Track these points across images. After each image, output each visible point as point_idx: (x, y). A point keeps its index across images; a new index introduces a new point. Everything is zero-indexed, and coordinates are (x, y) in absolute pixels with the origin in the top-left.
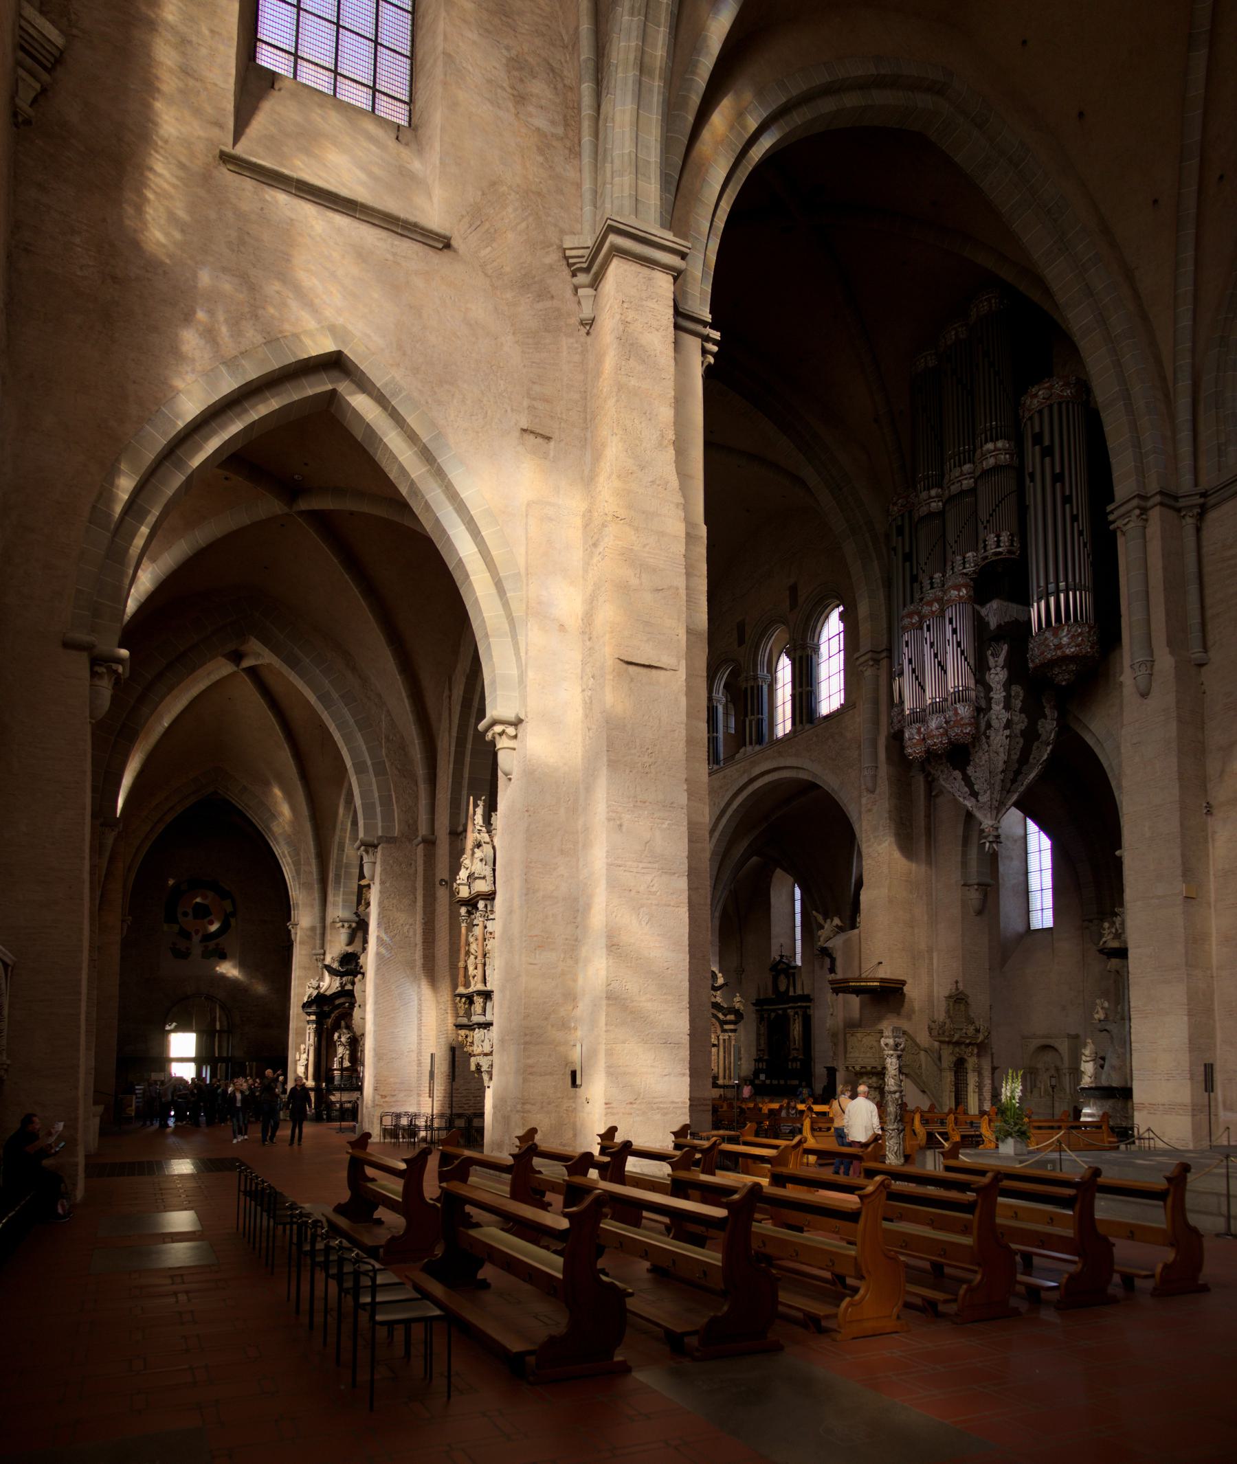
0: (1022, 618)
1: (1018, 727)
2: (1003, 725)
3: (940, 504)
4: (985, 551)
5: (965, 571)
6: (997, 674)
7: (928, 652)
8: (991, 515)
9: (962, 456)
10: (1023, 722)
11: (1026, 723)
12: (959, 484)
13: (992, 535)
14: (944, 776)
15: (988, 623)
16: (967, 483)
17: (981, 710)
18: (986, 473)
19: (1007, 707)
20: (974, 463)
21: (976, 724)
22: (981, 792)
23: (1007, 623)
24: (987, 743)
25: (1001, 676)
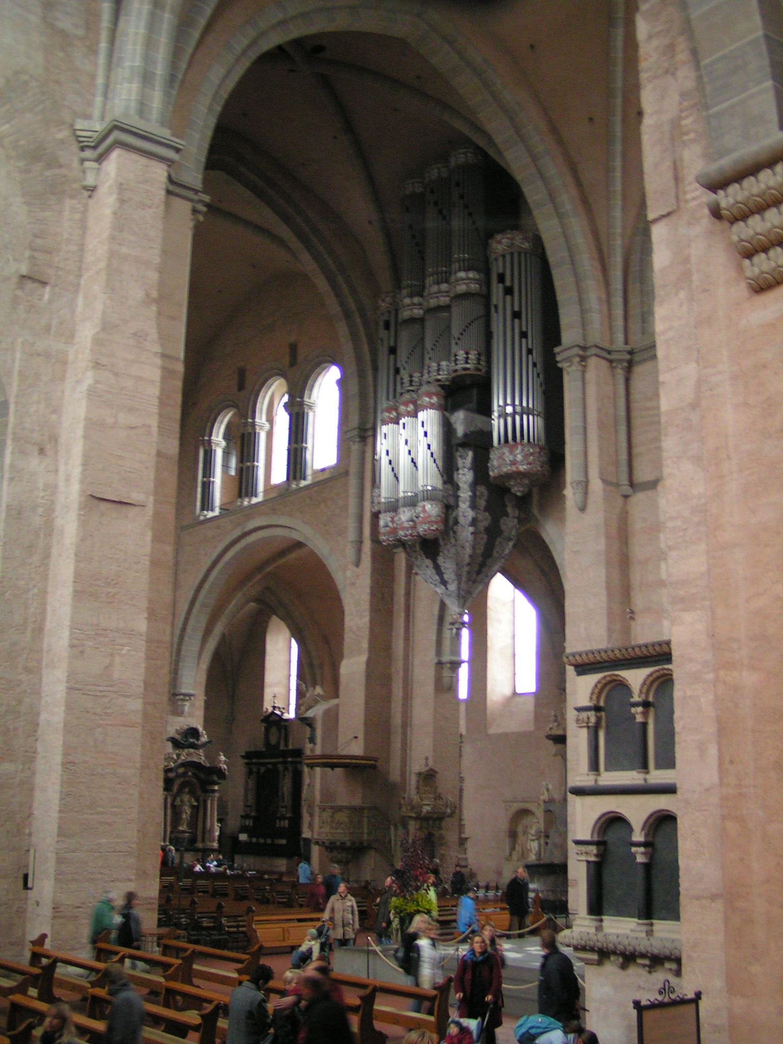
0: (486, 429)
3: (421, 312)
5: (439, 377)
6: (464, 474)
16: (444, 300)
17: (449, 508)
19: (473, 506)
22: (450, 581)
23: (473, 433)
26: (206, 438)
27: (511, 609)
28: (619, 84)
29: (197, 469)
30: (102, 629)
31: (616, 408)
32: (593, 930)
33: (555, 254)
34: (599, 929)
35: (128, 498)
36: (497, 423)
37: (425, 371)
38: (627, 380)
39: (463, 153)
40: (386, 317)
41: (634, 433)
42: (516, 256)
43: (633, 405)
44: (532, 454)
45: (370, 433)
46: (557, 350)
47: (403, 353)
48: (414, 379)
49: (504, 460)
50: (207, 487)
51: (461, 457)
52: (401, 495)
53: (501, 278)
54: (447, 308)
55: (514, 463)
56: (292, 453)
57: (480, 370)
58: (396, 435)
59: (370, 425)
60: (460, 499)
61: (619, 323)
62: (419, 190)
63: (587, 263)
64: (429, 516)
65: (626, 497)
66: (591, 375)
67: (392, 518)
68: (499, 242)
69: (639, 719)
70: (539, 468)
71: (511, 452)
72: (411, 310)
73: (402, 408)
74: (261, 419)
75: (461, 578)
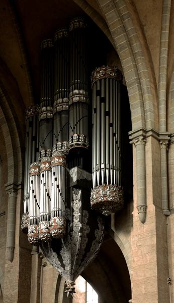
1: (86, 232)
5: (62, 150)
8: (76, 125)
10: (88, 230)
12: (61, 107)
13: (75, 135)
14: (49, 255)
15: (72, 178)
17: (68, 221)
18: (74, 104)
19: (81, 221)
20: (69, 98)
22: (67, 265)
36: (95, 176)
38: (167, 152)
40: (31, 120)
43: (170, 166)
44: (115, 191)
45: (20, 187)
46: (130, 133)
48: (47, 152)
51: (75, 193)
53: (99, 93)
55: (105, 196)
57: (86, 146)
59: (20, 183)
60: (74, 217)
65: (167, 216)
71: (103, 190)
75: (73, 264)
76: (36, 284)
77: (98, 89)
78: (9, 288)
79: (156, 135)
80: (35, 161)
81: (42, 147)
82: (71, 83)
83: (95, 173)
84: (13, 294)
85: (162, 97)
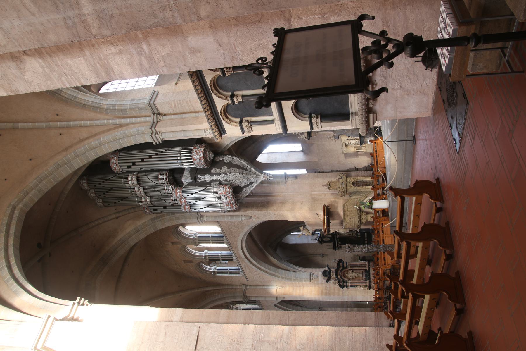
0: (189, 170)
1: (226, 170)
2: (226, 175)
3: (147, 197)
4: (165, 183)
5: (171, 190)
6: (207, 178)
7: (199, 203)
8: (153, 181)
9: (132, 191)
11: (225, 167)
13: (160, 181)
15: (190, 182)
16: (141, 189)
19: (219, 174)
21: (226, 185)
24: (232, 181)
25: (208, 176)
26: (213, 273)
27: (271, 154)
28: (44, 124)
29: (224, 276)
30: (253, 346)
31: (176, 119)
32: (357, 117)
33: (117, 146)
34: (356, 114)
35: (195, 335)
37: (170, 195)
38: (165, 115)
39: (83, 184)
41: (185, 111)
42: (120, 162)
43: (175, 112)
44: (196, 152)
46: (154, 144)
47: (165, 203)
49: (199, 162)
50: (231, 272)
51: (200, 180)
52: (217, 202)
53: (129, 167)
54: (144, 187)
56: (214, 242)
57: (166, 174)
58: (195, 206)
61: (143, 119)
62: (101, 200)
63: (118, 133)
64: (224, 191)
66: (163, 129)
67: (227, 205)
68: (115, 168)
69: (240, 99)
70: (202, 148)
71: (196, 160)
72: (147, 201)
73: (183, 204)
74: (204, 253)
76: (265, 198)
77: (126, 167)
78: (269, 217)
79: (154, 125)
80: (181, 208)
81: (170, 203)
82: (125, 186)
83: (185, 166)
84: (274, 214)
85: (127, 121)
